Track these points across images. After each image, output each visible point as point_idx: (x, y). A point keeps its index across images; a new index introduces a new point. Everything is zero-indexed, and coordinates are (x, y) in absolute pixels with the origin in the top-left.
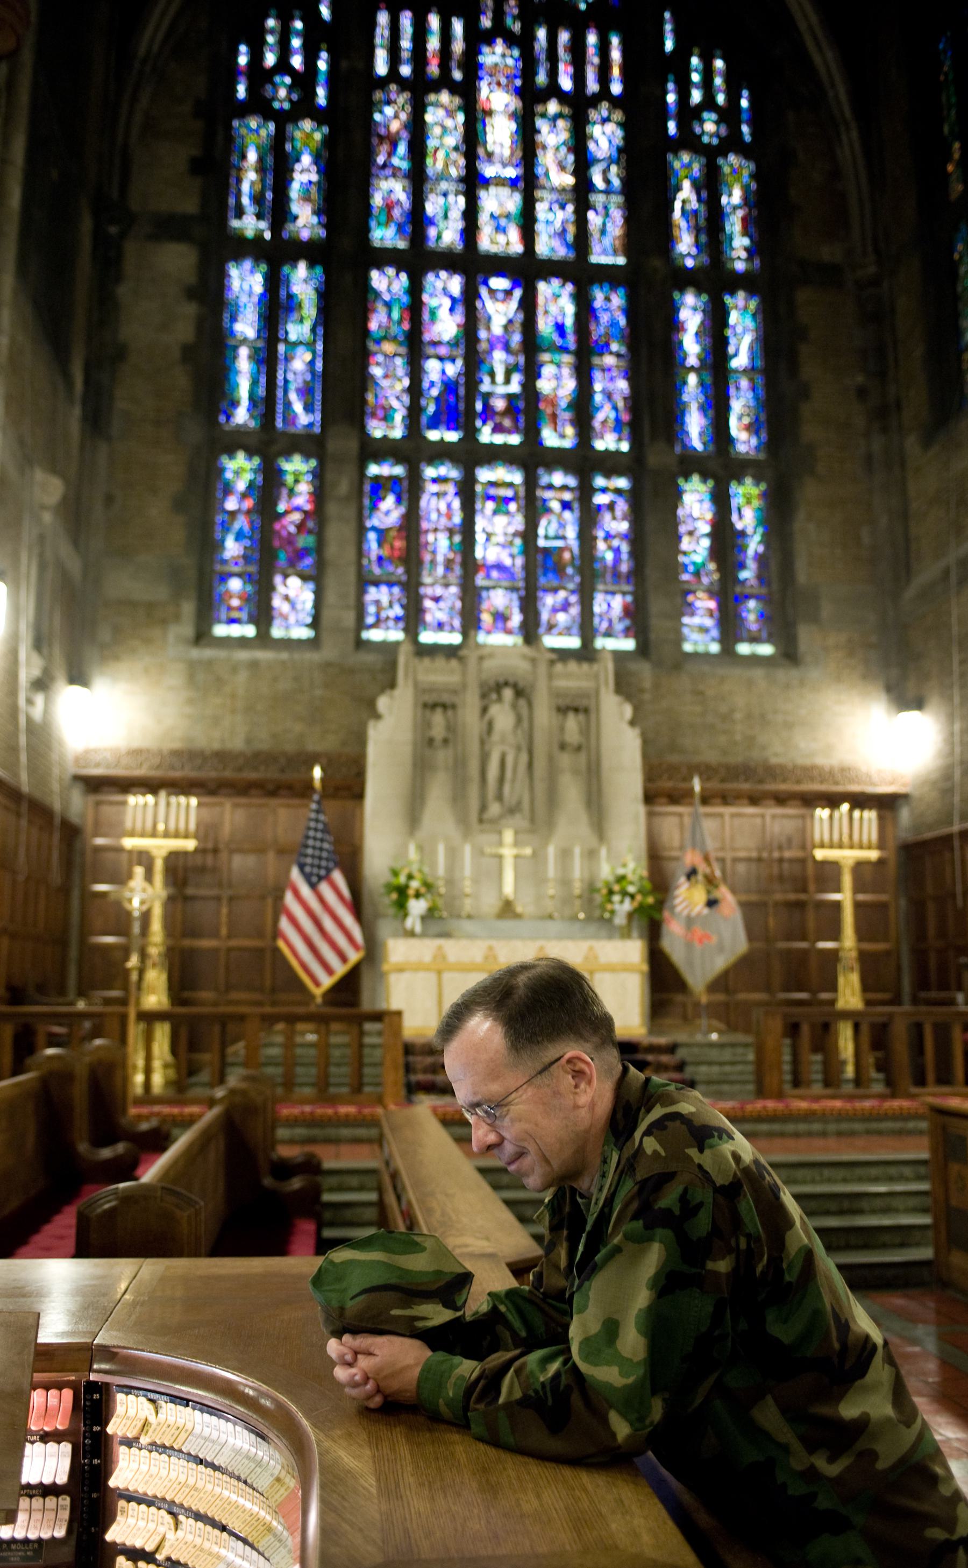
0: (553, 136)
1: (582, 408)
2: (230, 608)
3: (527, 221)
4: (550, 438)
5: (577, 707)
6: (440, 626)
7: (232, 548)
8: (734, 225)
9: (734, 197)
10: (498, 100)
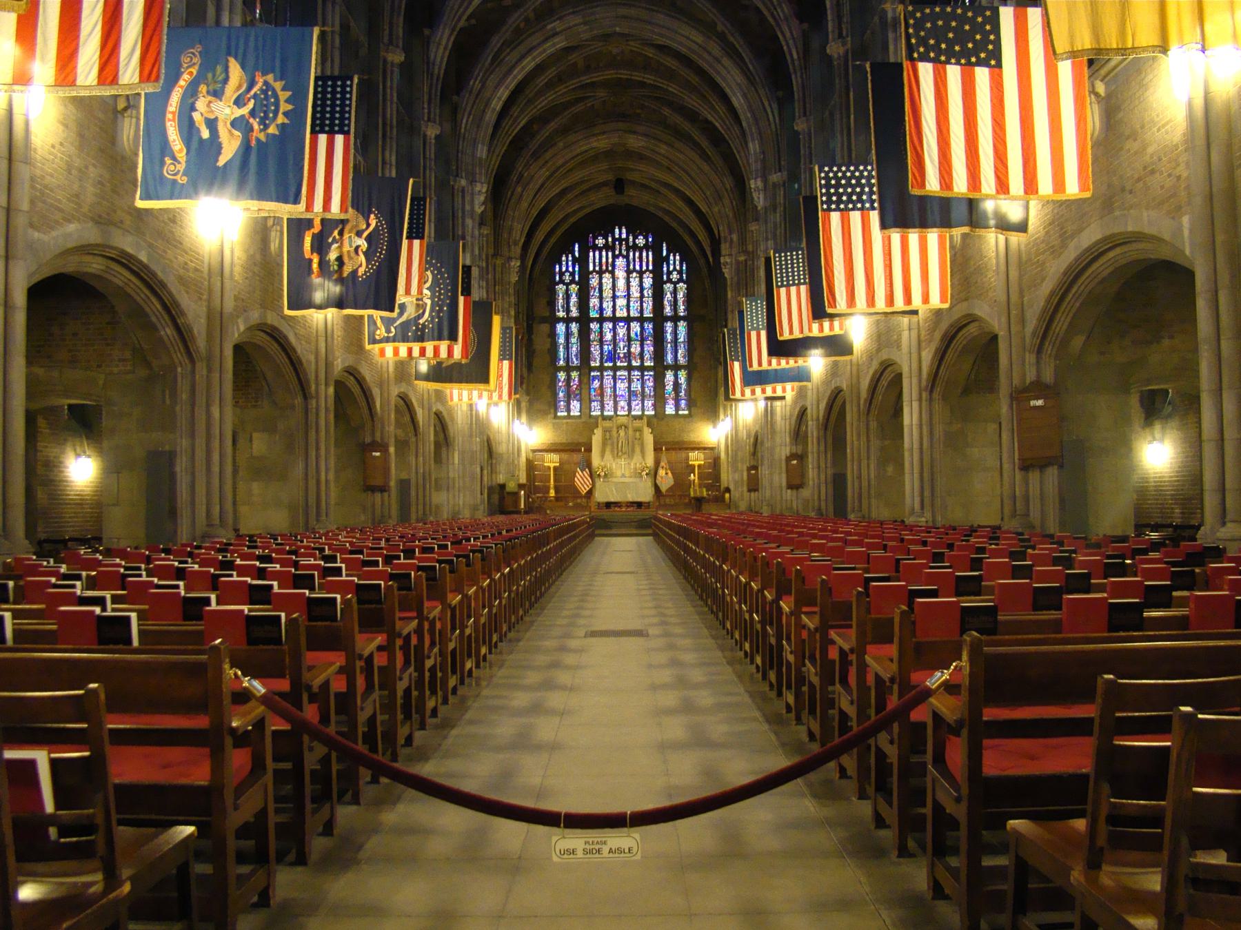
0: (634, 283)
4: (634, 363)
5: (640, 430)
7: (561, 395)
8: (680, 302)
9: (680, 296)
10: (621, 274)
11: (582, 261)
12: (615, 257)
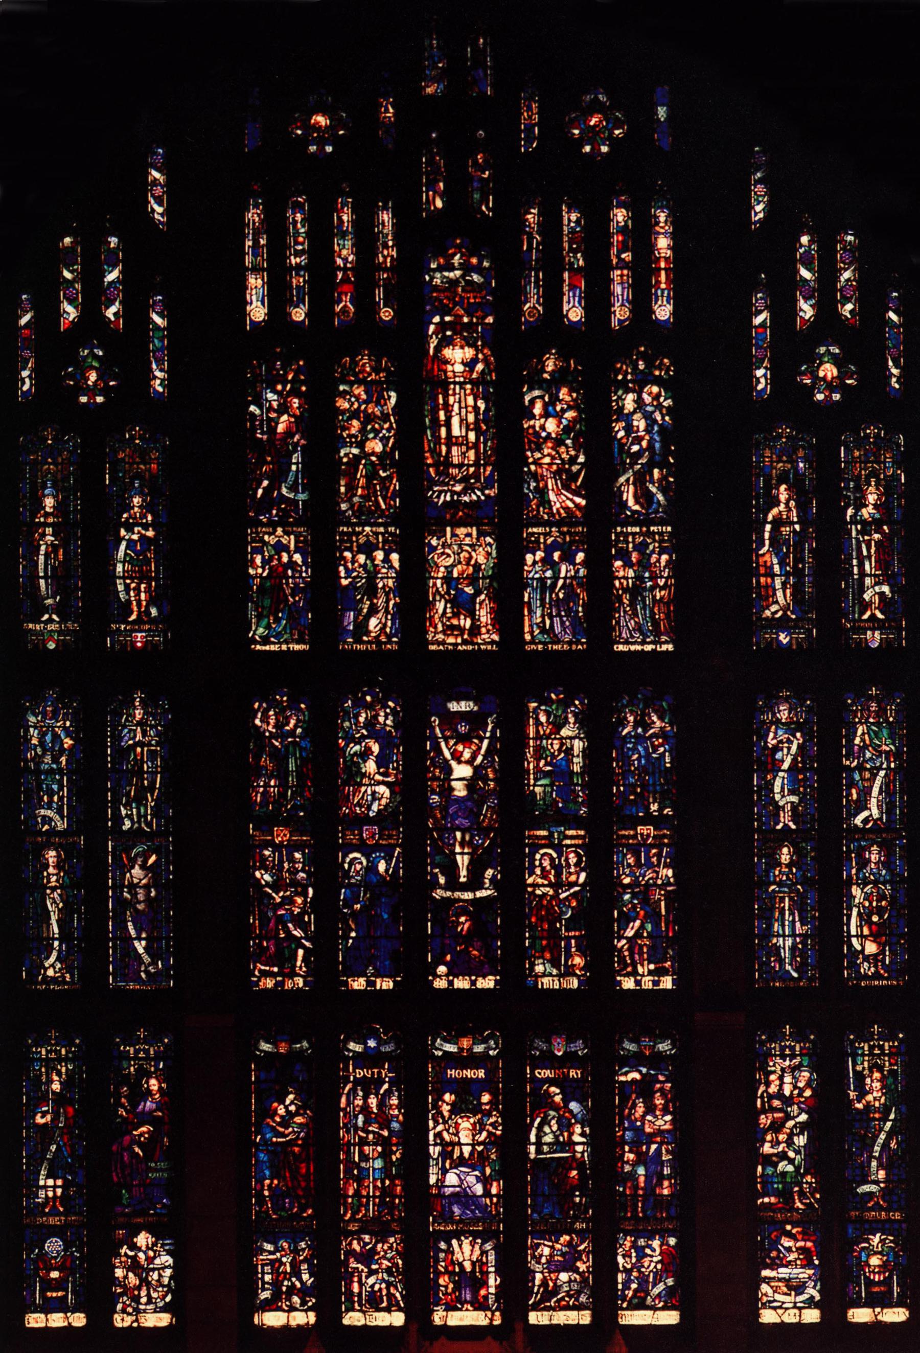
1: (598, 910)
2: (48, 1285)
3: (507, 585)
6: (374, 1302)
11: (193, 268)
12: (423, 238)
